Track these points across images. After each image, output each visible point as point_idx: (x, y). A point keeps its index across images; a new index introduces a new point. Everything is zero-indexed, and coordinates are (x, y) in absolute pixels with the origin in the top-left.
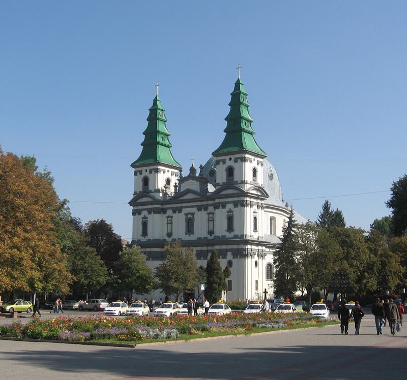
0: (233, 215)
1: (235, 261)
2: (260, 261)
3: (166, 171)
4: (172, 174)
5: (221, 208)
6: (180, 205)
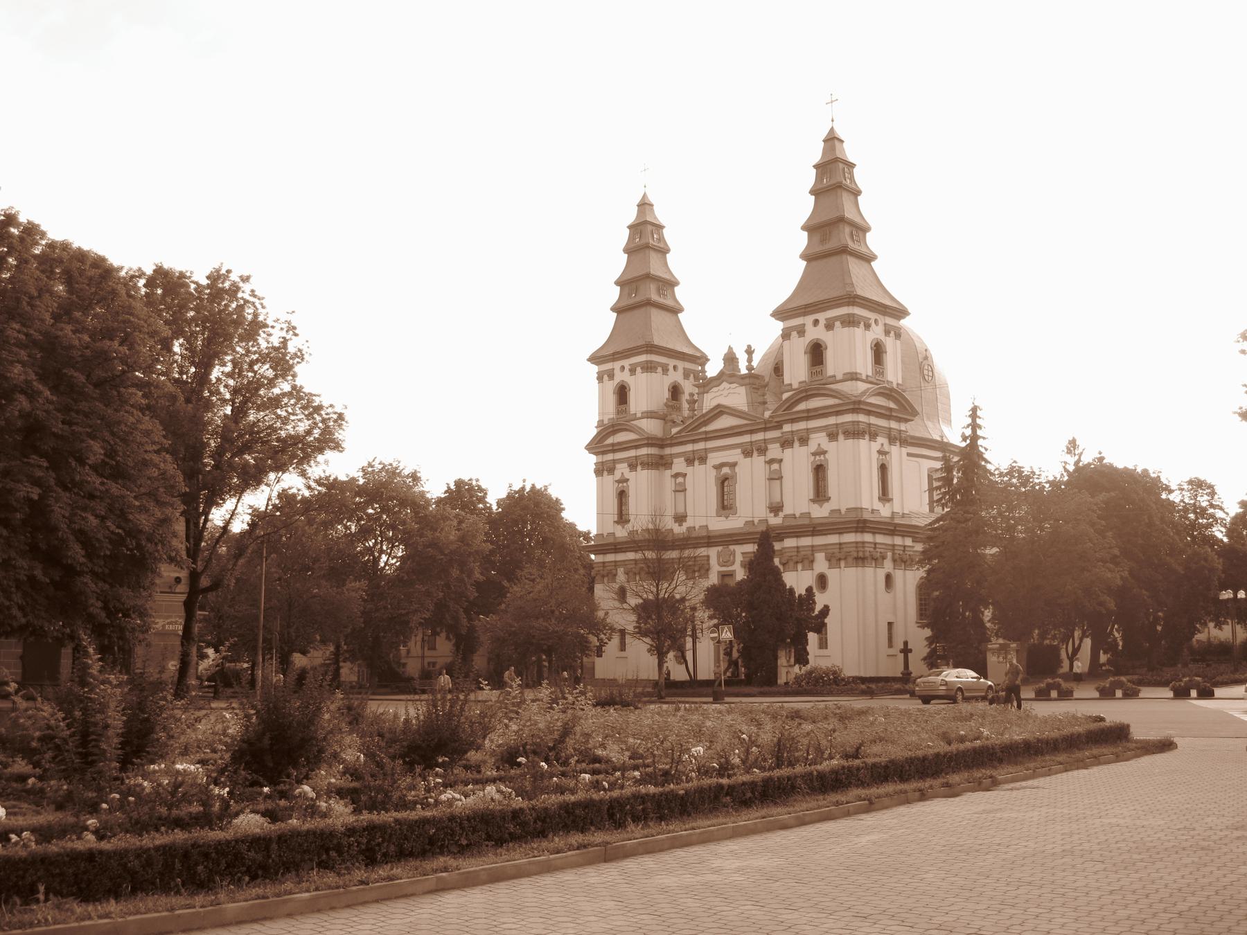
0: (826, 460)
1: (833, 575)
2: (898, 575)
3: (671, 368)
4: (686, 376)
5: (796, 444)
6: (701, 446)
